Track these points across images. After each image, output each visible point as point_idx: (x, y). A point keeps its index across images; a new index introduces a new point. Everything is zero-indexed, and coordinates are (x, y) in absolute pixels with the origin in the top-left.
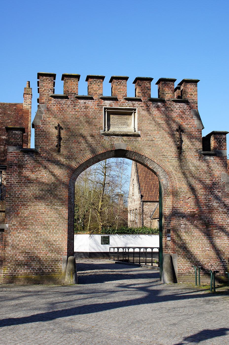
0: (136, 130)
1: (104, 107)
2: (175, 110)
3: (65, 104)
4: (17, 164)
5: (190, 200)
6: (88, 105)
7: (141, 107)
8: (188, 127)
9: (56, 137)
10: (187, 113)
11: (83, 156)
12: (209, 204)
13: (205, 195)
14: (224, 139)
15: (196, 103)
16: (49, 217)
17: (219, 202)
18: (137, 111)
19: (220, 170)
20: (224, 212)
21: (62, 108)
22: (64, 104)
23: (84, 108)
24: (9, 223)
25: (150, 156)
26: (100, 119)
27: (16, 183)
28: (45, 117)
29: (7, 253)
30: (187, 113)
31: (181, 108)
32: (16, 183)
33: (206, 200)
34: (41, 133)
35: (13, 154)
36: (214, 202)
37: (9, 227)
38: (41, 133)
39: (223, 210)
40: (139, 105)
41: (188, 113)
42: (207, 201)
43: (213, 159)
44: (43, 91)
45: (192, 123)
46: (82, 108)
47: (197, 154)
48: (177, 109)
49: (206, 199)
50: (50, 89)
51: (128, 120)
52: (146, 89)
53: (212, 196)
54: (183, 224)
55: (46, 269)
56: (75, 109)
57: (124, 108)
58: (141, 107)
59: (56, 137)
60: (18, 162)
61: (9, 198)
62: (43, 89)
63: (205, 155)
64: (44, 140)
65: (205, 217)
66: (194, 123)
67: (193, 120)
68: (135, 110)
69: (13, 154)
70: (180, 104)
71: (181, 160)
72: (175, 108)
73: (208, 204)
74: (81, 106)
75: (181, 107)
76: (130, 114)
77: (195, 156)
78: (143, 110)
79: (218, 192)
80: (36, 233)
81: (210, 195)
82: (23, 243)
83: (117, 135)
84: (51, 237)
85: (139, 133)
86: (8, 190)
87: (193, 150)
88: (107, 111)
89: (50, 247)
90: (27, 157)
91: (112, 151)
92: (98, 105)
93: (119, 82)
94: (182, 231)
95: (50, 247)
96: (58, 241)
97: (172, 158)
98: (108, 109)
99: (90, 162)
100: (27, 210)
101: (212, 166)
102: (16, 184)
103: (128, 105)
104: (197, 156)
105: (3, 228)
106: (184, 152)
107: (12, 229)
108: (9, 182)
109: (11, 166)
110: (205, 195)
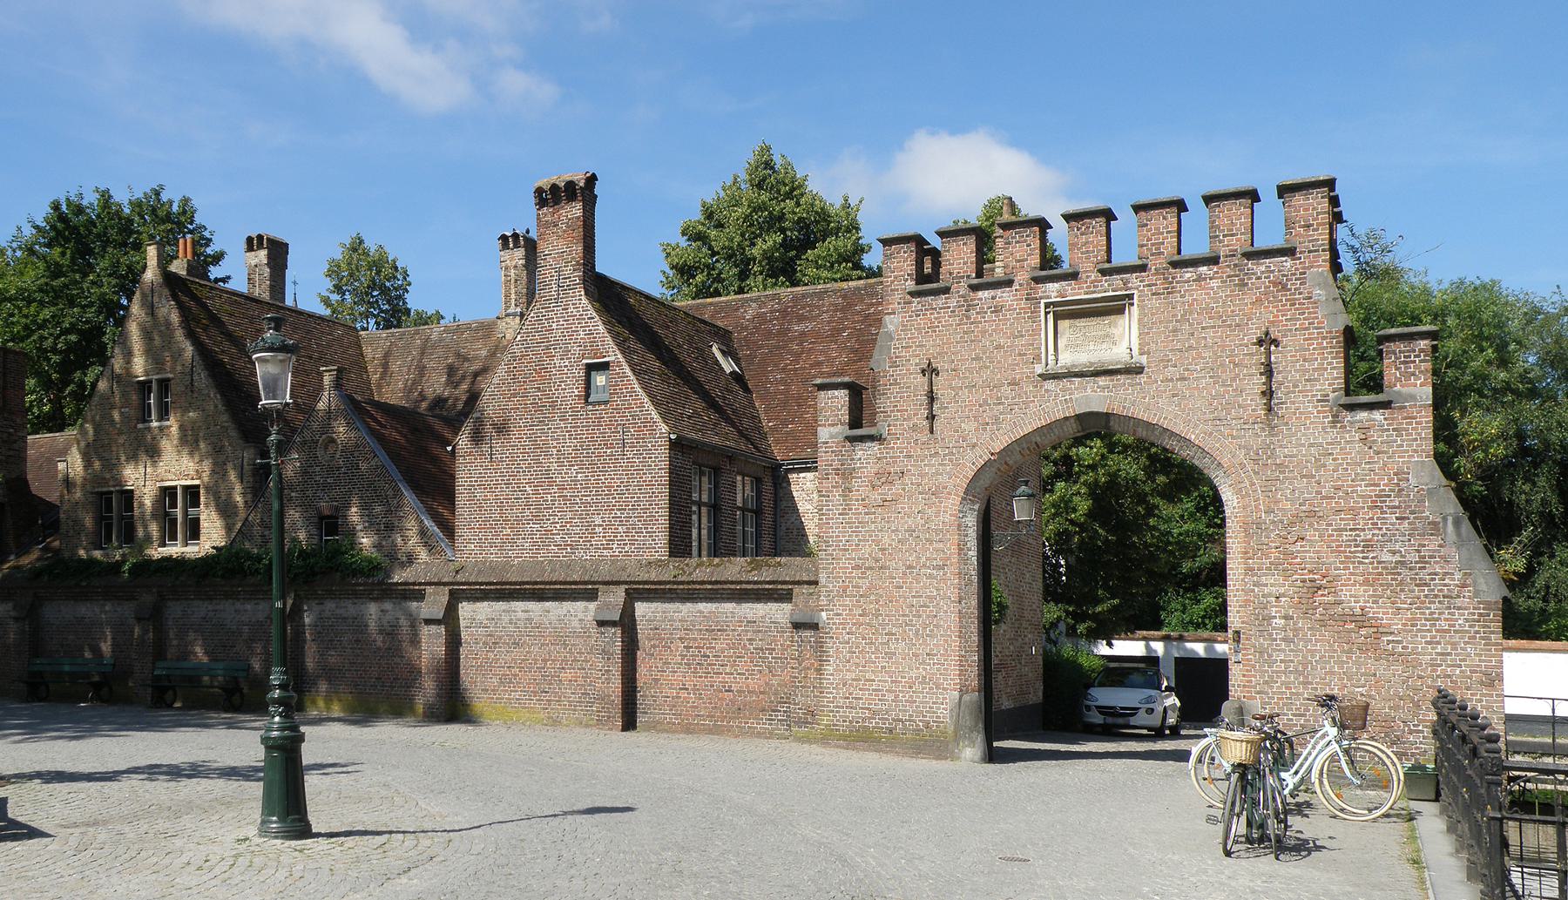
0: (1136, 352)
1: (1043, 301)
2: (1254, 281)
4: (838, 469)
5: (1301, 546)
6: (1003, 301)
7: (1149, 286)
8: (1297, 326)
9: (925, 395)
11: (991, 439)
12: (1367, 558)
13: (1351, 530)
17: (1401, 552)
18: (1136, 301)
21: (936, 318)
22: (941, 309)
23: (992, 312)
24: (827, 610)
25: (1175, 423)
27: (839, 514)
29: (825, 679)
31: (1272, 272)
32: (839, 514)
34: (890, 389)
36: (1385, 550)
37: (828, 619)
38: (890, 389)
39: (1417, 574)
41: (1297, 284)
42: (1360, 549)
43: (1382, 417)
44: (892, 282)
46: (986, 313)
49: (1356, 540)
51: (1115, 327)
52: (1163, 233)
53: (1376, 532)
54: (1277, 615)
55: (910, 721)
57: (1100, 295)
58: (1149, 286)
59: (925, 395)
62: (891, 277)
63: (1351, 408)
64: (897, 406)
65: (1351, 596)
67: (1311, 303)
68: (1131, 297)
70: (1268, 261)
71: (1273, 428)
72: (1253, 274)
74: (983, 308)
75: (1272, 268)
76: (1120, 311)
77: (1318, 412)
78: (1153, 294)
79: (1397, 518)
80: (886, 634)
81: (1370, 529)
82: (857, 657)
84: (920, 644)
85: (1144, 360)
86: (823, 532)
88: (1054, 312)
89: (918, 668)
91: (1066, 419)
94: (1275, 636)
95: (918, 668)
96: (936, 655)
97: (1245, 424)
98: (1053, 304)
99: (1012, 452)
100: (864, 578)
101: (1379, 439)
102: (839, 519)
103: (1109, 285)
104: (1325, 412)
105: (815, 621)
106: (1282, 403)
107: (834, 624)
108: (823, 514)
109: (826, 474)
110: (1351, 530)
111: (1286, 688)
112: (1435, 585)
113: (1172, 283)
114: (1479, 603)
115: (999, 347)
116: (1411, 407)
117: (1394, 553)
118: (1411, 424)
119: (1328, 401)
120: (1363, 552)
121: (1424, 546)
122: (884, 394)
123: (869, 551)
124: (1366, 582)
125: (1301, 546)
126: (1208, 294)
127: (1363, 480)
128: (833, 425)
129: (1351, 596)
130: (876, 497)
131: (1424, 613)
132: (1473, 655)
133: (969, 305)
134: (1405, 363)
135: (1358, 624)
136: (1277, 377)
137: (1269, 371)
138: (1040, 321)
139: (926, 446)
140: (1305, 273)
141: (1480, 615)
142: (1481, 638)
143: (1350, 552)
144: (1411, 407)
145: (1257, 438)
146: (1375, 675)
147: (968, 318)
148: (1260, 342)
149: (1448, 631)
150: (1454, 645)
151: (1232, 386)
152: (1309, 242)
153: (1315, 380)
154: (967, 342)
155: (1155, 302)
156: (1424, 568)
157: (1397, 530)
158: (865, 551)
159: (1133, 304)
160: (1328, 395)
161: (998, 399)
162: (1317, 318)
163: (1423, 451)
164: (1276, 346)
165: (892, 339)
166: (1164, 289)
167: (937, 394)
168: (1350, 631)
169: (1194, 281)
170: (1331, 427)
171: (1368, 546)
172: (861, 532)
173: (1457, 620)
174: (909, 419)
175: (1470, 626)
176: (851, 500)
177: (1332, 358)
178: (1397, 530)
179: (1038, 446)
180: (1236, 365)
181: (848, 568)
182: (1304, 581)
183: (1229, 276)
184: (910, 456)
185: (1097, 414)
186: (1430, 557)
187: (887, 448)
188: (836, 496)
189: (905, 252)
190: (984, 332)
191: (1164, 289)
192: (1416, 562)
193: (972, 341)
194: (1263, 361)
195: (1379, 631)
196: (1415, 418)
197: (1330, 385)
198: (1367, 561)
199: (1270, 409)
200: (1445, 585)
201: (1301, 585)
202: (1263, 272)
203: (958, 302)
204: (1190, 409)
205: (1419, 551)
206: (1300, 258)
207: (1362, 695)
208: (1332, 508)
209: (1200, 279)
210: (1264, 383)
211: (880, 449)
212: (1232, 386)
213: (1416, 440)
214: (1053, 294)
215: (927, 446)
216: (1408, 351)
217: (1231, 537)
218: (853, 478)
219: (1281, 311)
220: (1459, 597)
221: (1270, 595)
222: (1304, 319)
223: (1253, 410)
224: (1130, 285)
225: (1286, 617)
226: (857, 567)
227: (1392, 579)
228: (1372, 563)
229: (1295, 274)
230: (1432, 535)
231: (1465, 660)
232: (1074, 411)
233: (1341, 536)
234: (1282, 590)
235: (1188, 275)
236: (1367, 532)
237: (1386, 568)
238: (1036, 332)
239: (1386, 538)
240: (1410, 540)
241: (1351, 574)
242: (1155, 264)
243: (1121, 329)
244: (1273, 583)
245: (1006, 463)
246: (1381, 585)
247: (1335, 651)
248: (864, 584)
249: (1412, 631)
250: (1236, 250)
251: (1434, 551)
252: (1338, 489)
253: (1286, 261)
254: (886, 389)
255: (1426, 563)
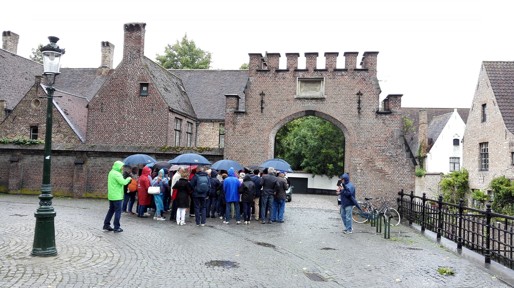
3: (268, 76)
4: (232, 122)
5: (366, 150)
6: (286, 76)
7: (328, 76)
9: (261, 101)
10: (367, 79)
12: (383, 154)
13: (379, 147)
14: (399, 100)
15: (375, 71)
16: (254, 161)
18: (324, 80)
19: (394, 126)
20: (396, 160)
21: (265, 79)
22: (267, 76)
25: (334, 115)
26: (295, 87)
27: (231, 135)
28: (253, 87)
30: (367, 79)
31: (362, 75)
32: (231, 135)
33: (380, 151)
35: (229, 115)
39: (395, 159)
40: (326, 74)
45: (371, 87)
47: (374, 113)
48: (358, 77)
50: (257, 65)
52: (333, 61)
53: (386, 147)
56: (275, 80)
57: (314, 77)
58: (328, 76)
59: (261, 101)
60: (233, 120)
61: (226, 146)
65: (378, 164)
66: (373, 87)
67: (372, 85)
69: (229, 115)
70: (361, 72)
71: (360, 118)
72: (357, 75)
73: (382, 154)
75: (362, 74)
76: (320, 82)
78: (329, 78)
79: (391, 144)
81: (384, 147)
83: (307, 99)
85: (326, 96)
87: (371, 110)
90: (239, 116)
91: (303, 111)
92: (293, 76)
93: (310, 56)
100: (238, 155)
103: (317, 75)
104: (374, 114)
106: (363, 111)
110: (379, 147)
111: (360, 189)
112: (400, 162)
113: (334, 76)
114: (410, 167)
115: (284, 89)
116: (396, 115)
117: (390, 153)
118: (395, 119)
119: (375, 111)
120: (382, 152)
121: (397, 151)
122: (248, 100)
123: (240, 146)
124: (382, 161)
125: (366, 150)
126: (344, 80)
127: (383, 133)
128: (231, 108)
129: (378, 164)
130: (244, 130)
131: (397, 169)
132: (408, 180)
133: (275, 76)
134: (395, 103)
135: (380, 172)
136: (361, 104)
137: (359, 102)
138: (296, 83)
139: (260, 117)
140: (370, 77)
141: (410, 170)
142: (410, 176)
143: (379, 152)
144: (396, 115)
145: (355, 120)
146: (384, 185)
147: (275, 80)
148: (358, 94)
149: (402, 174)
150: (404, 178)
151: (349, 105)
152: (372, 68)
153: (372, 106)
154: (274, 87)
155: (330, 81)
156: (397, 157)
157: (391, 147)
158: (239, 147)
159: (323, 81)
160: (375, 110)
161: (283, 104)
162: (373, 89)
163: (398, 126)
164: (362, 96)
165: (251, 84)
166: (333, 77)
167: (264, 101)
168: (377, 174)
169: (341, 76)
170: (375, 119)
171: (383, 151)
172: (238, 141)
173: (405, 171)
174: (255, 108)
175: (408, 173)
176: (235, 131)
177: (376, 100)
178: (391, 147)
179: (293, 119)
180: (351, 100)
181: (233, 152)
182: (366, 160)
183: (350, 75)
184: (255, 119)
185: (312, 111)
186: (399, 154)
187: (248, 116)
188: (231, 130)
189: (256, 58)
190: (280, 84)
191: (333, 77)
192: (395, 156)
193: (276, 87)
194: (358, 99)
195: (385, 174)
196: (396, 118)
197: (375, 107)
198: (383, 155)
199: (359, 113)
200: (402, 162)
201: (366, 161)
202: (359, 75)
203: (272, 75)
204: (338, 111)
205: (396, 153)
206: (369, 72)
207: (380, 191)
208: (374, 140)
209: (342, 75)
210: (358, 106)
211: (246, 116)
212: (349, 105)
213: (396, 123)
214: (301, 76)
215: (260, 117)
216: (396, 100)
217: (347, 147)
218: (236, 124)
219: (364, 86)
220: (405, 165)
221: (357, 163)
222: (370, 89)
223: (355, 113)
224: (323, 75)
225: (361, 170)
226: (236, 151)
227: (389, 160)
228: (384, 156)
229: (368, 77)
230: (399, 149)
231: (406, 182)
232: (305, 109)
233: (376, 148)
234: (360, 162)
235: (339, 74)
236: (383, 147)
237: (388, 157)
238: (295, 86)
239: (388, 149)
240: (394, 150)
241: (379, 158)
242: (330, 70)
243: (319, 87)
244: (358, 160)
245: (284, 123)
246: (386, 161)
247: (374, 179)
248: (239, 157)
249: (393, 174)
250: (352, 68)
251: (400, 153)
252: (376, 135)
253: (366, 73)
254: (248, 99)
255: (398, 156)
